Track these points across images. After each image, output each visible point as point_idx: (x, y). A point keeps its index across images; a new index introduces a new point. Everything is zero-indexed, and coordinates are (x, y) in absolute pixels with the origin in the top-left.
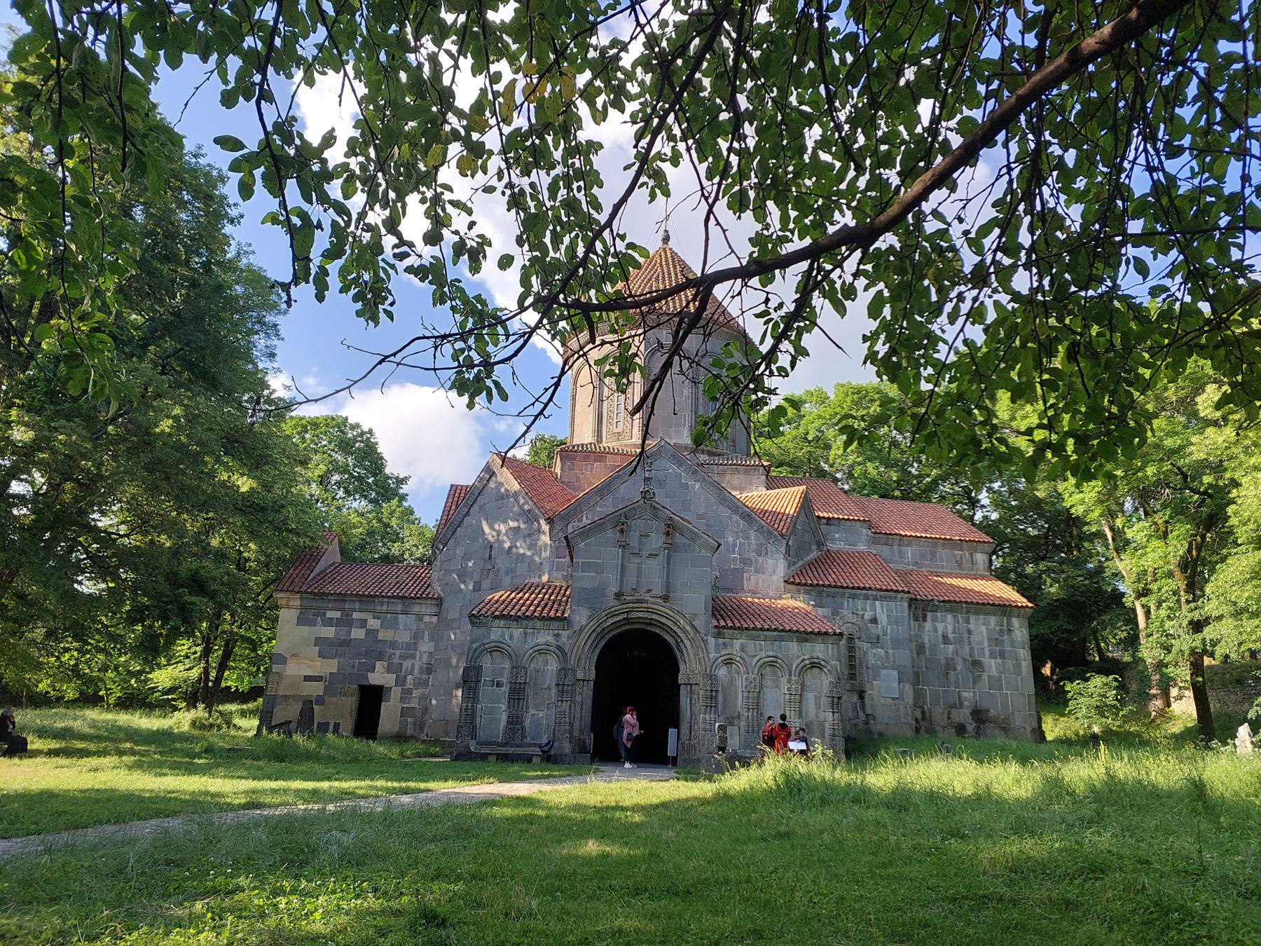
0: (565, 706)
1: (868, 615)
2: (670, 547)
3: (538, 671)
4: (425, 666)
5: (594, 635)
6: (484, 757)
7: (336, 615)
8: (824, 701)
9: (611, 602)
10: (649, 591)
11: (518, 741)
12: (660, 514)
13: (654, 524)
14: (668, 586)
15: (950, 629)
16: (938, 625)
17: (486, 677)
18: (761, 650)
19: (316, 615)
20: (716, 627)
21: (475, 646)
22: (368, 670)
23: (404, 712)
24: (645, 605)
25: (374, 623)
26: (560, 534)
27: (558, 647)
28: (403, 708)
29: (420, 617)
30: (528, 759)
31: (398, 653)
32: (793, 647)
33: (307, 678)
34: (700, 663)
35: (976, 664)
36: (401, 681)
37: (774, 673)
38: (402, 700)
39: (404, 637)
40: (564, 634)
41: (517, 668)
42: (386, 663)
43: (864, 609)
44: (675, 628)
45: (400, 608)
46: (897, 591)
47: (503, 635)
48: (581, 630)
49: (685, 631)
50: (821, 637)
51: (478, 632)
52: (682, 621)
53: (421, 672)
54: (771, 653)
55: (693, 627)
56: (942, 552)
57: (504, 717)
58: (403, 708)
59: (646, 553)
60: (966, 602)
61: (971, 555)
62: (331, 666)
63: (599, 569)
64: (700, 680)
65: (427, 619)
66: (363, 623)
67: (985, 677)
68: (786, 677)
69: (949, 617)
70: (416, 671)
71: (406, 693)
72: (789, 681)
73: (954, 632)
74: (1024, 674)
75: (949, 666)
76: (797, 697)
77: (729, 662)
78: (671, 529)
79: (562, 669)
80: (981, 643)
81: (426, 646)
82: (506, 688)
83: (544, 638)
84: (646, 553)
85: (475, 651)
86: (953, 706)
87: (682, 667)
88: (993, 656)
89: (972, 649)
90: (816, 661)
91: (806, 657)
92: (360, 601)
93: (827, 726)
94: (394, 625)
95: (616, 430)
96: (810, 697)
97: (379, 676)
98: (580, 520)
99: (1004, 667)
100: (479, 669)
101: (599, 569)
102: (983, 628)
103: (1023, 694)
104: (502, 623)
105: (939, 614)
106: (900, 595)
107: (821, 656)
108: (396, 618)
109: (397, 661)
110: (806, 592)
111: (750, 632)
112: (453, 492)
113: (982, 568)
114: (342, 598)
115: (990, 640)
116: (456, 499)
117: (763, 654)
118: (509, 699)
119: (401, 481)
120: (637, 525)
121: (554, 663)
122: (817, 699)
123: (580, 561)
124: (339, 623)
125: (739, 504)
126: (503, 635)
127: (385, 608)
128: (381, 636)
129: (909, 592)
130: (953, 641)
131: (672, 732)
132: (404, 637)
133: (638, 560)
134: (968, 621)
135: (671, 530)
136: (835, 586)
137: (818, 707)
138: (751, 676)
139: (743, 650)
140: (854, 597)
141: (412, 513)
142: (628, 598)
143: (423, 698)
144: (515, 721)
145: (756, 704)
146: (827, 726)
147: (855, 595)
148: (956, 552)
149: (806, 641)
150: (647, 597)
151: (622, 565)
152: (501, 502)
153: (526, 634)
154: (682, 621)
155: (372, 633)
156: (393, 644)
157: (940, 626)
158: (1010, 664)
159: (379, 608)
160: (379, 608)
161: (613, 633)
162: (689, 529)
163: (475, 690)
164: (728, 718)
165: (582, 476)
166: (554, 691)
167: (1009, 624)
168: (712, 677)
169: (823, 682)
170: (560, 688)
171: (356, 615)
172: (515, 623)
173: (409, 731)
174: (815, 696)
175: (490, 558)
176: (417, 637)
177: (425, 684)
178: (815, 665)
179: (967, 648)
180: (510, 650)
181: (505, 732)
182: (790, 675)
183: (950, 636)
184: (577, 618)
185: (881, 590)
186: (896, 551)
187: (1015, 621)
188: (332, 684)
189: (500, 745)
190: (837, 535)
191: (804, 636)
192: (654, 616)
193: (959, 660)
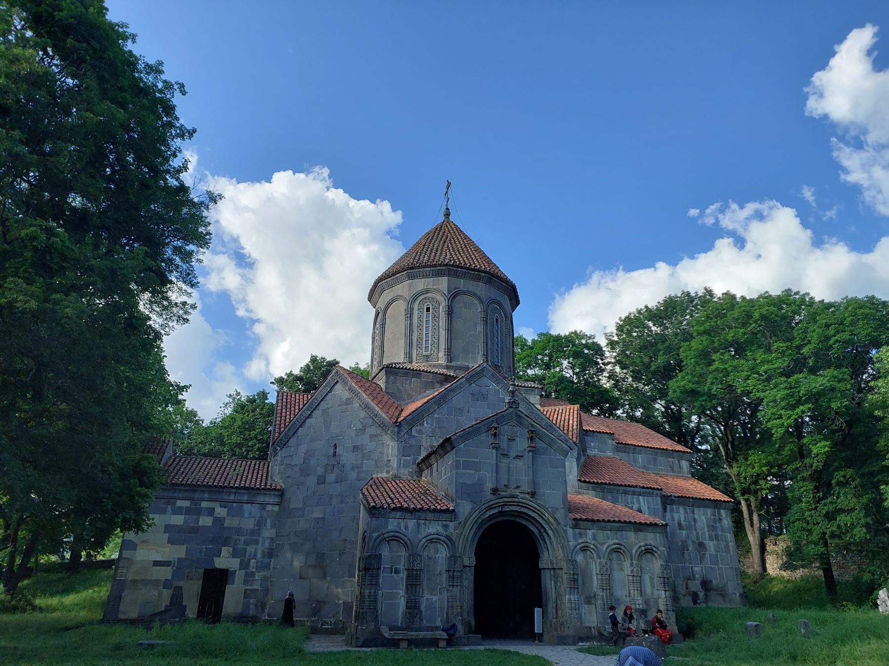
0: (456, 590)
1: (636, 506)
2: (534, 451)
3: (430, 558)
4: (267, 550)
5: (476, 525)
6: (393, 643)
7: (185, 504)
8: (656, 580)
9: (488, 495)
10: (518, 487)
12: (524, 422)
13: (518, 430)
14: (534, 483)
15: (682, 519)
16: (674, 515)
17: (385, 565)
18: (608, 539)
19: (168, 504)
20: (575, 519)
21: (375, 535)
22: (214, 555)
23: (247, 594)
24: (516, 500)
25: (220, 511)
26: (406, 436)
27: (447, 537)
28: (246, 590)
29: (263, 505)
30: (434, 643)
31: (243, 539)
32: (631, 535)
33: (156, 563)
34: (563, 551)
35: (701, 545)
36: (244, 565)
37: (619, 559)
38: (246, 582)
39: (248, 524)
40: (452, 524)
41: (413, 556)
42: (231, 549)
43: (632, 503)
44: (540, 520)
45: (245, 498)
46: (654, 488)
47: (399, 526)
48: (466, 521)
49: (548, 522)
50: (651, 528)
51: (375, 522)
52: (546, 514)
53: (263, 556)
54: (616, 541)
55: (555, 519)
56: (661, 459)
57: (402, 603)
58: (246, 590)
59: (513, 454)
60: (692, 498)
61: (679, 461)
62: (179, 552)
63: (476, 466)
64: (564, 565)
65: (269, 508)
66: (211, 512)
67: (707, 556)
68: (627, 564)
69: (681, 509)
70: (259, 555)
71: (249, 576)
72: (632, 565)
73: (685, 521)
74: (732, 553)
75: (684, 547)
76: (638, 578)
77: (585, 549)
78: (533, 435)
79: (452, 556)
80: (702, 529)
81: (268, 532)
82: (403, 575)
83: (434, 528)
84: (513, 454)
85: (375, 540)
87: (546, 553)
88: (711, 539)
89: (697, 533)
90: (649, 547)
91: (642, 544)
92: (210, 492)
94: (239, 513)
95: (424, 353)
96: (647, 577)
97: (224, 561)
98: (422, 424)
99: (719, 547)
100: (379, 557)
101: (476, 466)
102: (703, 517)
103: (732, 568)
104: (399, 514)
105: (674, 507)
106: (655, 492)
107: (653, 544)
108: (242, 506)
109: (241, 546)
110: (594, 489)
111: (600, 523)
112: (280, 398)
113: (686, 471)
114: (193, 488)
115: (708, 526)
116: (284, 404)
117: (611, 542)
118: (407, 585)
119: (182, 389)
120: (506, 430)
121: (443, 550)
122: (652, 579)
123: (461, 459)
124: (188, 511)
125: (543, 416)
126: (399, 526)
127: (232, 497)
128: (227, 523)
129: (661, 490)
130: (685, 527)
131: (538, 611)
132: (248, 524)
133: (506, 461)
134: (693, 513)
135: (534, 435)
136: (614, 484)
137: (653, 587)
138: (603, 561)
139: (594, 539)
140: (625, 493)
141: (195, 416)
142: (503, 494)
143: (264, 580)
144: (413, 606)
145: (608, 584)
147: (626, 491)
148: (670, 459)
149: (641, 530)
150: (517, 492)
151: (497, 465)
152: (345, 407)
153: (418, 525)
154: (546, 514)
155: (219, 521)
156: (239, 531)
157: (676, 516)
158: (722, 544)
159: (226, 497)
160: (226, 497)
161: (488, 524)
162: (547, 435)
163: (377, 577)
164: (587, 598)
165: (402, 389)
166: (445, 576)
167: (719, 514)
168: (573, 562)
169: (656, 565)
170: (451, 574)
171: (204, 504)
172: (409, 514)
173: (252, 612)
174: (650, 577)
175: (335, 454)
176: (260, 523)
177: (267, 567)
178: (649, 551)
179: (694, 533)
180: (406, 539)
182: (632, 560)
183: (683, 523)
184: (462, 511)
185: (643, 487)
186: (631, 458)
187: (722, 512)
188: (180, 567)
189: (401, 629)
190: (592, 444)
191: (639, 527)
192: (523, 510)
193: (690, 542)
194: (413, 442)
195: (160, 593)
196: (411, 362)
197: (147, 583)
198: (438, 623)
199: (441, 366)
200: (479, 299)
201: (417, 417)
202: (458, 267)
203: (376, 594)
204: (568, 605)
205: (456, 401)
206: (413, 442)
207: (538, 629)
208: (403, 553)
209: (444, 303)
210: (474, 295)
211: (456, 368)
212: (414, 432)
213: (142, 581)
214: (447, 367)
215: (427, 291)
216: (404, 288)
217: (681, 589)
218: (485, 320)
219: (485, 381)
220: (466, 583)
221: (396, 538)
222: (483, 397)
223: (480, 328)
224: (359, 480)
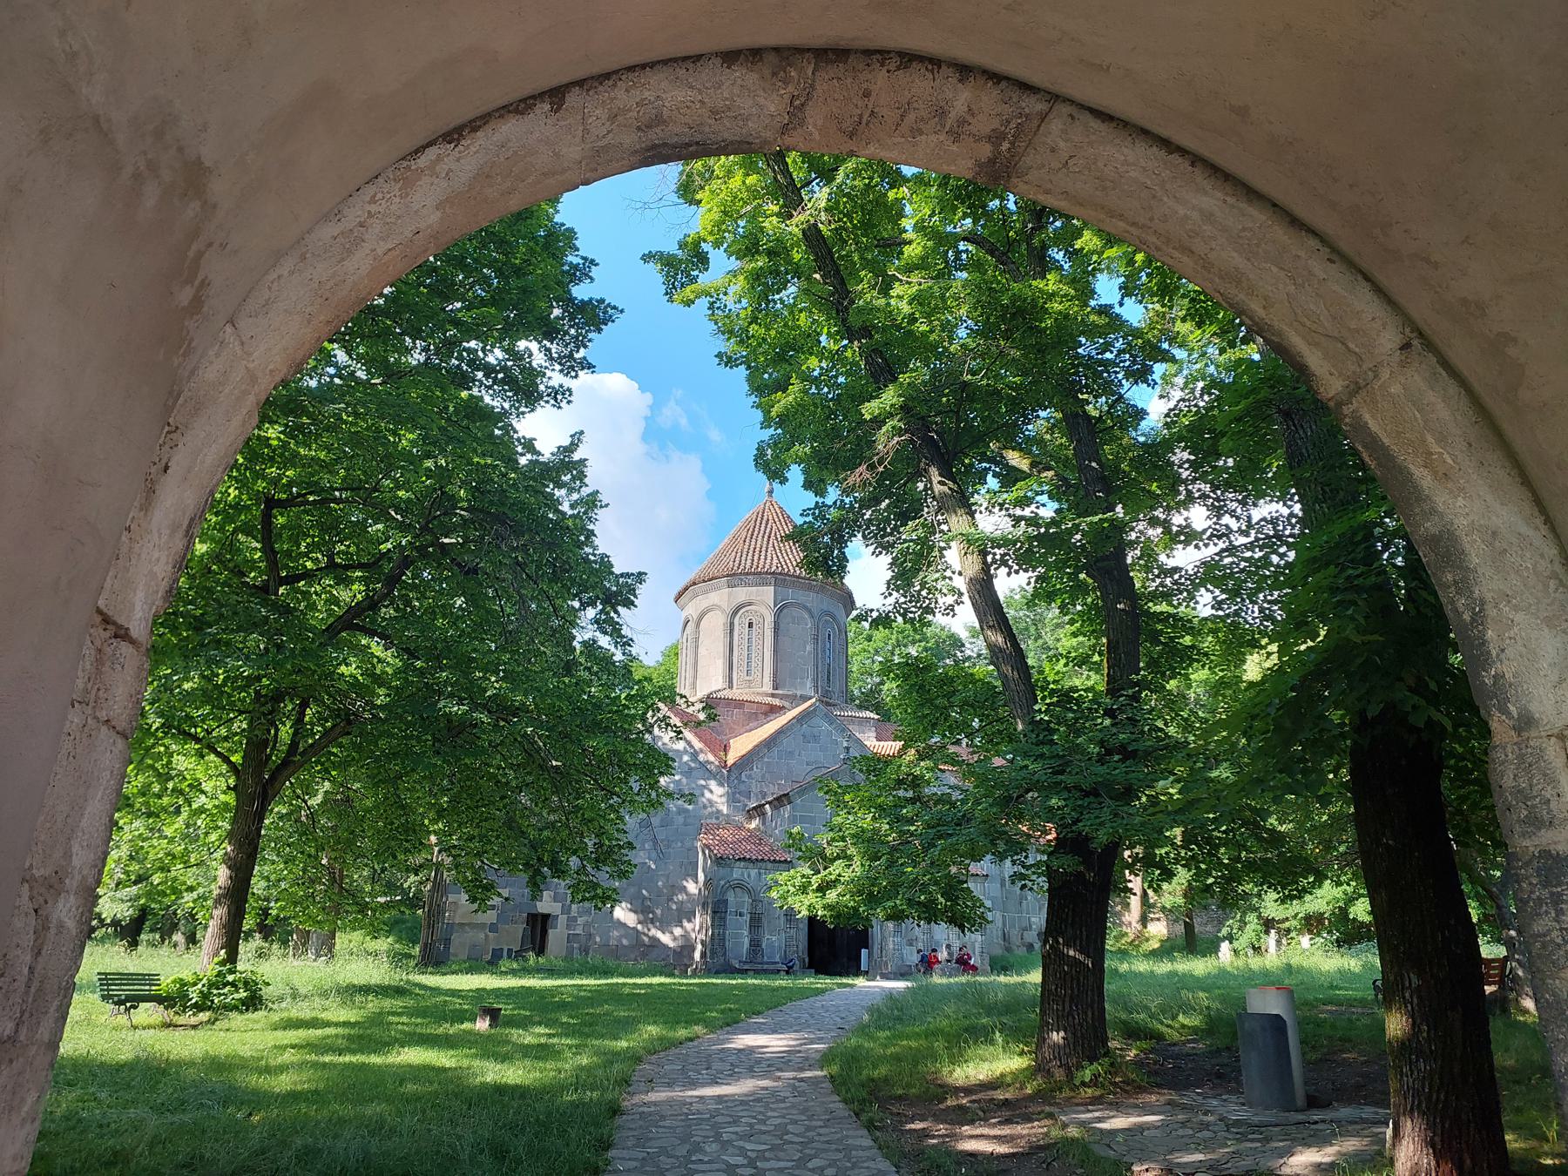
11: (759, 960)
17: (731, 909)
21: (722, 883)
23: (570, 938)
51: (722, 871)
57: (746, 941)
71: (572, 921)
82: (747, 918)
86: (1025, 929)
93: (977, 945)
131: (864, 952)
144: (755, 944)
146: (977, 945)
163: (724, 919)
166: (783, 919)
181: (749, 952)
194: (742, 787)
195: (486, 936)
196: (731, 687)
198: (777, 959)
199: (767, 695)
200: (809, 611)
201: (746, 761)
202: (787, 575)
203: (724, 934)
206: (742, 787)
208: (746, 898)
209: (769, 619)
210: (805, 608)
211: (782, 697)
212: (744, 778)
213: (469, 924)
214: (773, 695)
215: (750, 604)
216: (721, 597)
217: (1016, 940)
219: (817, 721)
220: (801, 926)
221: (740, 886)
222: (815, 738)
223: (809, 648)
224: (685, 824)
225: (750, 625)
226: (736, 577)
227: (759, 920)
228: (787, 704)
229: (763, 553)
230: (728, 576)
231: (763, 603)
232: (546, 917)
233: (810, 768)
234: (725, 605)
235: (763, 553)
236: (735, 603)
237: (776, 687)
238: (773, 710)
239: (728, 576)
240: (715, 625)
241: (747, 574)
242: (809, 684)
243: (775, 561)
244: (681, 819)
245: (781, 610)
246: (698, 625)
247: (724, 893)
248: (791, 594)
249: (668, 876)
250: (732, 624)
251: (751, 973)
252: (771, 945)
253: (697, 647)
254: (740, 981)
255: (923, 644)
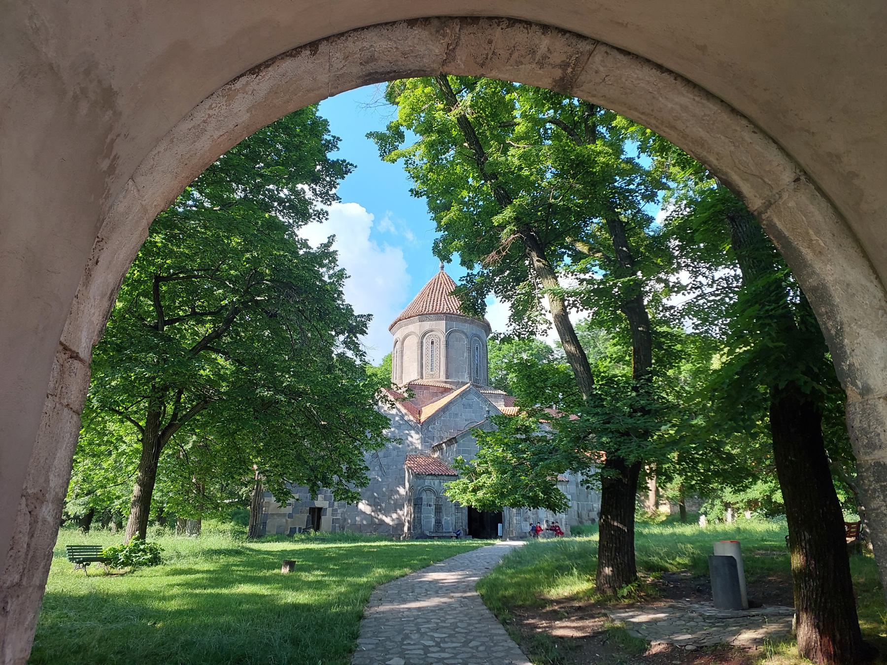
0: (459, 515)
11: (440, 531)
17: (424, 503)
21: (419, 488)
38: (333, 515)
57: (433, 520)
71: (334, 512)
82: (433, 507)
86: (590, 511)
93: (563, 521)
98: (435, 424)
131: (500, 525)
144: (438, 522)
146: (563, 521)
166: (454, 508)
181: (435, 525)
194: (430, 434)
195: (287, 521)
196: (422, 378)
197: (279, 515)
198: (451, 530)
200: (465, 334)
201: (432, 419)
202: (452, 314)
203: (420, 517)
204: (515, 522)
205: (453, 408)
207: (499, 534)
209: (443, 339)
210: (463, 332)
211: (451, 383)
212: (430, 429)
213: (277, 514)
214: (446, 382)
215: (432, 331)
216: (415, 327)
217: (585, 517)
218: (469, 349)
220: (464, 511)
222: (470, 406)
224: (398, 456)
225: (432, 343)
226: (423, 316)
227: (440, 508)
228: (454, 387)
229: (439, 302)
230: (419, 315)
231: (439, 330)
232: (320, 509)
233: (467, 423)
234: (417, 332)
235: (439, 302)
236: (423, 331)
237: (447, 377)
238: (446, 391)
239: (419, 315)
240: (412, 343)
241: (430, 314)
242: (466, 375)
243: (446, 306)
244: (395, 453)
245: (449, 334)
246: (403, 344)
247: (420, 493)
248: (455, 325)
249: (388, 485)
250: (422, 342)
251: (436, 538)
252: (447, 522)
253: (402, 356)
254: (430, 543)
255: (530, 352)
